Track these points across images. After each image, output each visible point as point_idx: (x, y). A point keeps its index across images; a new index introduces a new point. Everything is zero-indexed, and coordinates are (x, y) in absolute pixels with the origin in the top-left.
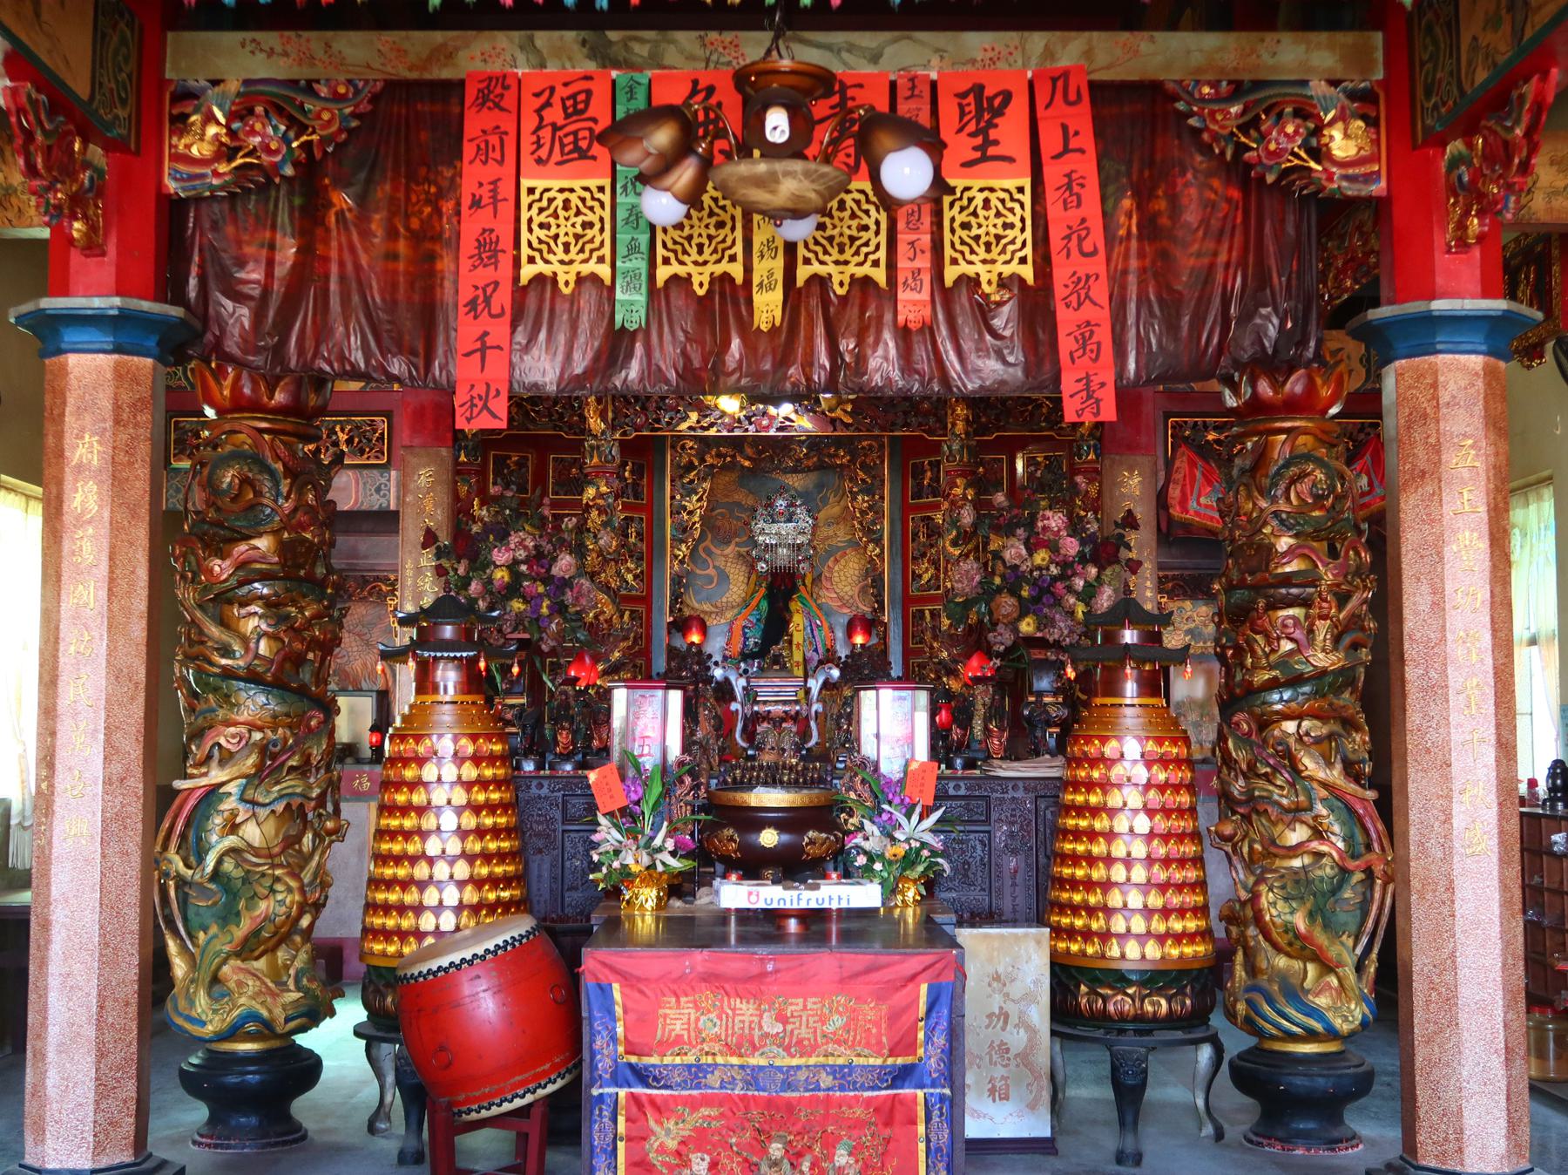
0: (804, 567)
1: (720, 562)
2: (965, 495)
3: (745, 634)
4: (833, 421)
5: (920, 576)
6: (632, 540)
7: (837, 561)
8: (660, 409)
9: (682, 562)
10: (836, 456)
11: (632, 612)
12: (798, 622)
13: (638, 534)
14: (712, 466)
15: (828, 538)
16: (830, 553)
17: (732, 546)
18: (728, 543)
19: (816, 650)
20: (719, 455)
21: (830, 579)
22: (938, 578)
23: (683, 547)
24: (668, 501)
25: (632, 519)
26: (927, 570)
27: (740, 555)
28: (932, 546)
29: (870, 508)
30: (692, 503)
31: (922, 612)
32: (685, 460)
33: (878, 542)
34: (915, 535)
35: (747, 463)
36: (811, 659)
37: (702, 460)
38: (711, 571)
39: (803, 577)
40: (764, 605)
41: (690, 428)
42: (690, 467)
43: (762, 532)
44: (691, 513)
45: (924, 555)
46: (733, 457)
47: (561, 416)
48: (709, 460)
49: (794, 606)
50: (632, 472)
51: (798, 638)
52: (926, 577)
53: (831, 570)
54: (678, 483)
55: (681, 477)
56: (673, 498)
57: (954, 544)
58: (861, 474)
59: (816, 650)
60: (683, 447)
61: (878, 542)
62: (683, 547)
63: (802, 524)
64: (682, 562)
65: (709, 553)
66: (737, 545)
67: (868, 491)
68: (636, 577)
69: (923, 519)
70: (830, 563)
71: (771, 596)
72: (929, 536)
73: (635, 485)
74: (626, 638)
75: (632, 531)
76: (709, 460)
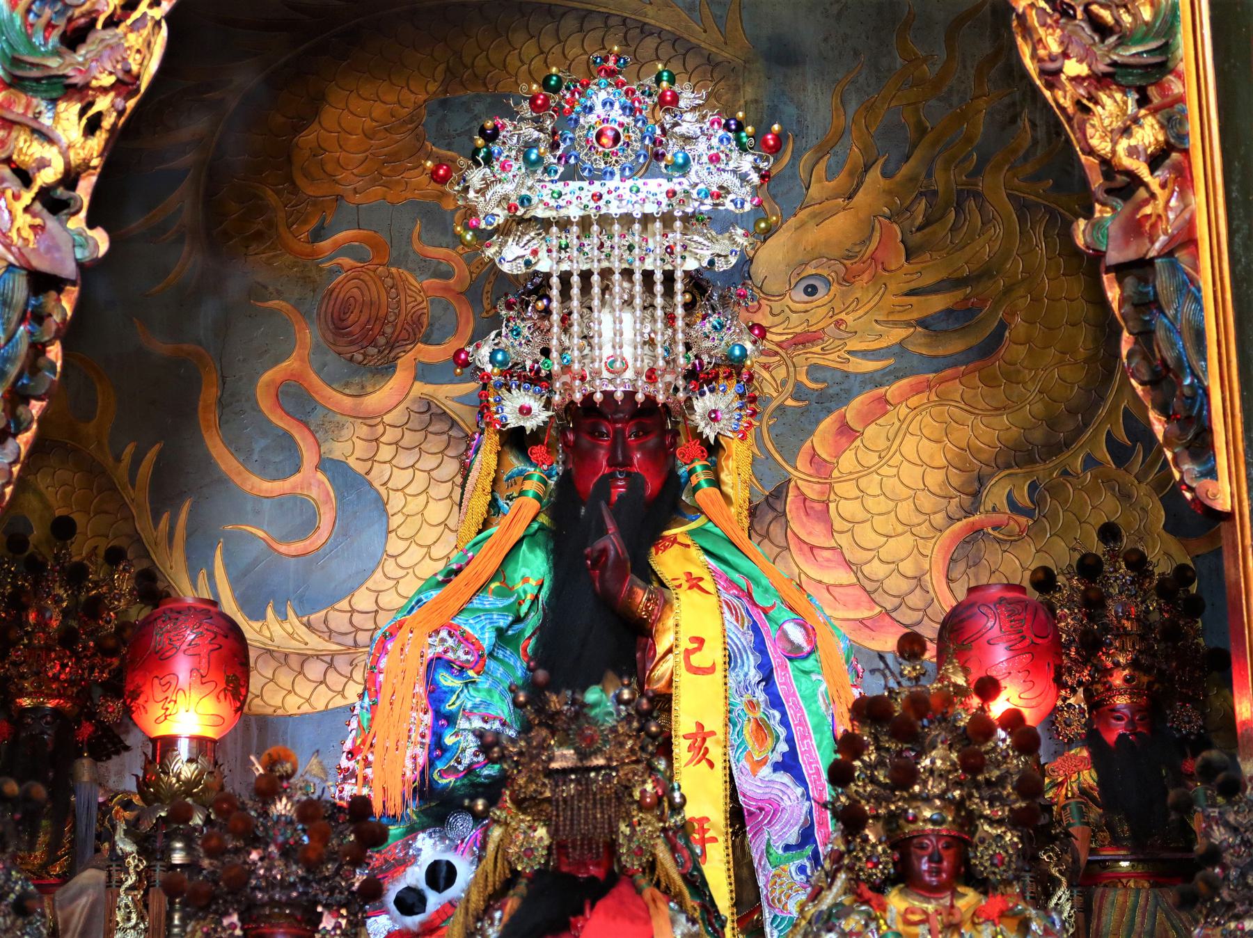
0: (713, 408)
1: (349, 447)
3: (435, 696)
7: (846, 432)
9: (53, 202)
12: (694, 625)
15: (803, 340)
16: (825, 396)
18: (386, 369)
19: (789, 764)
21: (821, 513)
23: (67, 121)
27: (432, 413)
33: (1147, 78)
36: (770, 809)
38: (312, 483)
39: (713, 449)
40: (533, 570)
43: (520, 222)
49: (670, 563)
51: (697, 704)
59: (789, 764)
61: (1147, 78)
62: (67, 121)
64: (53, 202)
65: (298, 400)
66: (424, 372)
70: (822, 437)
71: (566, 528)
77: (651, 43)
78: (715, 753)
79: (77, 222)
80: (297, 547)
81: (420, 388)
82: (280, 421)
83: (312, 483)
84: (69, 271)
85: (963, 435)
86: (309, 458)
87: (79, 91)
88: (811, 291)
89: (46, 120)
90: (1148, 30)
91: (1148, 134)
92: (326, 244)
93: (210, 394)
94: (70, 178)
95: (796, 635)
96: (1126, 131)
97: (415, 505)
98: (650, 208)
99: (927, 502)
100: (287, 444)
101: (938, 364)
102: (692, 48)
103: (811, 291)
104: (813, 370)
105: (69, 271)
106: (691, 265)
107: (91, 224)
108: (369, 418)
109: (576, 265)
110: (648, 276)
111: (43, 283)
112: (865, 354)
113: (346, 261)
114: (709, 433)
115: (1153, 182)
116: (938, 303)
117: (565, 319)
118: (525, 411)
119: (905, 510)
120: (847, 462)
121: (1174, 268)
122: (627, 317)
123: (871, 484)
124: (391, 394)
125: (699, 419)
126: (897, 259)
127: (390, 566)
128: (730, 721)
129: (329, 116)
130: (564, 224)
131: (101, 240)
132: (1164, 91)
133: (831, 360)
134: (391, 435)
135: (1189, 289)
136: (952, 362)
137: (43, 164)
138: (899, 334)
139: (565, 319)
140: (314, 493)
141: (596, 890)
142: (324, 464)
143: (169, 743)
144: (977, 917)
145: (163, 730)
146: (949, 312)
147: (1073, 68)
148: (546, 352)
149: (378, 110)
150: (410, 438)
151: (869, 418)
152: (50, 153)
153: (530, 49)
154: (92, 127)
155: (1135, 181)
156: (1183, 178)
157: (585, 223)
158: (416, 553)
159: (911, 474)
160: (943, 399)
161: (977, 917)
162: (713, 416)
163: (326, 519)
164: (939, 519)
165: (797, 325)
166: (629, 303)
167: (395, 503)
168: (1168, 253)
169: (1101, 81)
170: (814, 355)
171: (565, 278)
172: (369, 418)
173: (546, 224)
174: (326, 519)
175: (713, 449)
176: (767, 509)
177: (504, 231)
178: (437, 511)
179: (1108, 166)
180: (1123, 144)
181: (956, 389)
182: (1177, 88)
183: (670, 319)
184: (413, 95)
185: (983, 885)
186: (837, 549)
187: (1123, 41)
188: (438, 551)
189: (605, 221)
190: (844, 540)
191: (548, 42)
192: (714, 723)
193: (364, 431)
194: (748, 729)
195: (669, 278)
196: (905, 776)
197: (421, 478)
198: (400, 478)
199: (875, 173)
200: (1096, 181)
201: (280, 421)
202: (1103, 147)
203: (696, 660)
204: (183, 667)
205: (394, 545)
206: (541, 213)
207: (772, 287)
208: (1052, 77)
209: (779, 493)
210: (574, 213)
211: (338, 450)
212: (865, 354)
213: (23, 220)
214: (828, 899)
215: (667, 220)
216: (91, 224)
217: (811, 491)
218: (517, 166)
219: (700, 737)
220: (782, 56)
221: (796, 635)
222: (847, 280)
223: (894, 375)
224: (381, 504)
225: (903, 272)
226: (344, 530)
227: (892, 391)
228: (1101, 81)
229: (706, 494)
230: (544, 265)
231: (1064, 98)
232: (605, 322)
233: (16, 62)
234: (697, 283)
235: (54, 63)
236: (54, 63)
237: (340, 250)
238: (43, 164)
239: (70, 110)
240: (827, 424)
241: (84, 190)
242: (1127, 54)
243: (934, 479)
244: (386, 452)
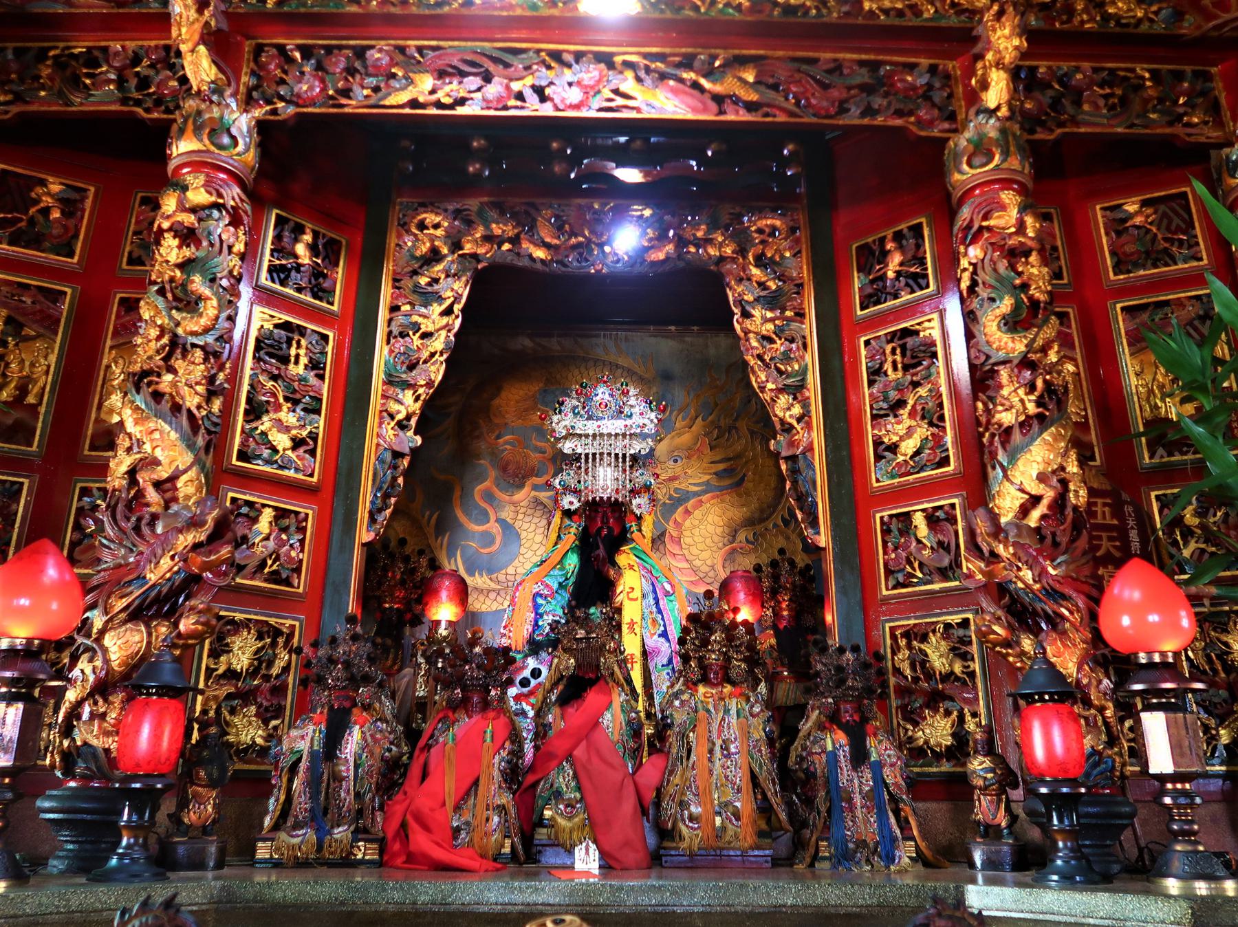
0: (640, 504)
1: (507, 514)
2: (1021, 227)
3: (536, 606)
4: (718, 99)
5: (893, 448)
6: (297, 370)
8: (350, 71)
9: (402, 426)
10: (708, 241)
11: (281, 514)
12: (631, 583)
13: (315, 365)
14: (475, 256)
16: (680, 499)
17: (526, 489)
18: (522, 486)
19: (664, 635)
20: (488, 238)
21: (678, 542)
22: (938, 441)
23: (408, 397)
24: (383, 314)
25: (302, 331)
26: (910, 432)
27: (538, 503)
28: (915, 385)
29: (779, 332)
30: (431, 319)
31: (907, 517)
32: (424, 248)
33: (796, 390)
34: (876, 373)
35: (540, 254)
36: (657, 652)
37: (456, 246)
39: (639, 519)
40: (573, 561)
41: (414, 103)
42: (434, 256)
43: (570, 435)
44: (426, 335)
45: (901, 403)
46: (515, 241)
47: (144, 83)
48: (468, 248)
49: (622, 560)
50: (313, 249)
51: (631, 612)
52: (908, 447)
53: (678, 525)
54: (407, 283)
55: (415, 273)
56: (394, 309)
57: (1013, 323)
58: (755, 271)
59: (664, 635)
60: (422, 226)
61: (796, 390)
62: (408, 397)
63: (637, 420)
64: (402, 426)
66: (535, 488)
67: (772, 301)
68: (297, 443)
69: (892, 337)
70: (678, 514)
71: (585, 546)
72: (906, 368)
73: (317, 273)
74: (195, 523)
75: (300, 352)
76: (468, 248)
77: (620, 371)
78: (637, 630)
79: (410, 433)
80: (487, 550)
81: (533, 493)
82: (484, 505)
83: (493, 527)
84: (407, 451)
85: (730, 514)
86: (493, 518)
87: (413, 386)
88: (676, 461)
89: (400, 396)
90: (797, 373)
91: (797, 410)
92: (501, 441)
93: (457, 493)
94: (408, 417)
95: (668, 587)
96: (789, 409)
97: (531, 536)
98: (618, 431)
99: (716, 539)
100: (486, 514)
101: (721, 489)
102: (635, 373)
103: (676, 461)
104: (676, 490)
105: (407, 451)
106: (632, 452)
107: (415, 434)
108: (514, 504)
109: (591, 451)
110: (617, 455)
111: (397, 455)
112: (695, 484)
113: (508, 447)
114: (638, 512)
115: (799, 428)
116: (721, 467)
117: (586, 470)
118: (571, 503)
119: (708, 541)
120: (688, 523)
121: (805, 458)
122: (609, 469)
123: (696, 532)
124: (523, 495)
125: (634, 507)
126: (707, 450)
127: (521, 558)
128: (643, 618)
129: (504, 394)
130: (587, 436)
131: (419, 440)
132: (802, 394)
133: (682, 486)
134: (523, 510)
135: (811, 466)
136: (726, 488)
137: (399, 412)
138: (708, 477)
139: (586, 470)
140: (494, 531)
141: (592, 683)
142: (497, 520)
143: (438, 623)
144: (731, 695)
145: (435, 618)
146: (725, 470)
147: (770, 386)
148: (579, 482)
149: (521, 393)
150: (529, 512)
151: (696, 507)
152: (401, 408)
153: (576, 372)
154: (417, 399)
155: (792, 427)
156: (809, 426)
157: (594, 436)
158: (530, 553)
159: (711, 528)
160: (723, 501)
161: (731, 695)
162: (639, 506)
163: (498, 540)
164: (720, 545)
165: (670, 473)
166: (610, 465)
167: (523, 535)
168: (803, 453)
169: (780, 391)
170: (676, 484)
171: (587, 455)
172: (514, 504)
173: (580, 436)
174: (498, 540)
175: (639, 519)
176: (658, 540)
177: (565, 438)
178: (539, 538)
179: (782, 421)
180: (788, 414)
181: (728, 497)
182: (807, 394)
183: (624, 471)
184: (535, 387)
185: (733, 683)
186: (683, 555)
187: (788, 377)
188: (539, 553)
189: (602, 435)
190: (686, 552)
191: (583, 370)
192: (637, 619)
193: (513, 508)
194: (649, 621)
195: (624, 456)
196: (705, 643)
197: (533, 526)
198: (525, 526)
199: (700, 419)
200: (778, 427)
201: (484, 505)
202: (781, 414)
203: (631, 596)
204: (444, 595)
205: (523, 550)
206: (578, 432)
207: (662, 459)
208: (763, 389)
209: (663, 534)
210: (591, 432)
211: (503, 515)
212: (695, 484)
213: (391, 432)
214: (677, 687)
215: (624, 435)
216: (415, 434)
217: (674, 534)
218: (570, 415)
219: (632, 624)
220: (667, 377)
221: (668, 587)
222: (689, 457)
223: (705, 492)
224: (518, 535)
225: (709, 455)
226: (505, 543)
227: (704, 498)
228: (780, 391)
229: (636, 535)
230: (579, 451)
231: (767, 397)
232: (601, 471)
233: (390, 375)
234: (635, 458)
235: (404, 376)
236: (404, 376)
237: (506, 443)
238: (399, 412)
239: (409, 393)
240: (681, 509)
241: (413, 422)
242: (789, 381)
243: (719, 530)
244: (520, 516)
